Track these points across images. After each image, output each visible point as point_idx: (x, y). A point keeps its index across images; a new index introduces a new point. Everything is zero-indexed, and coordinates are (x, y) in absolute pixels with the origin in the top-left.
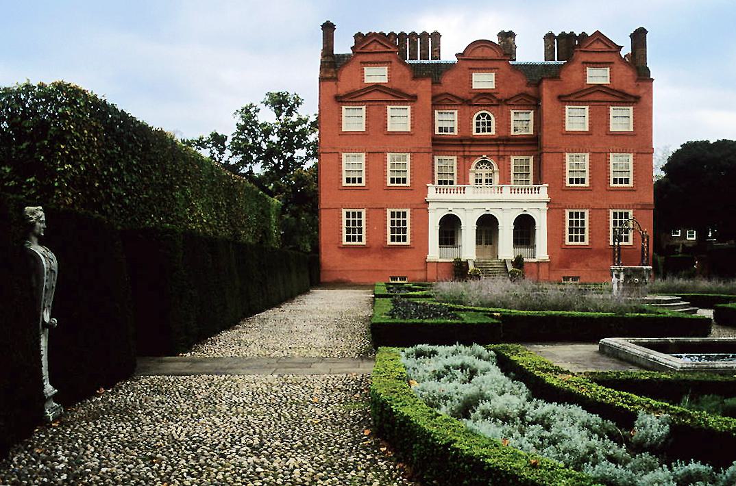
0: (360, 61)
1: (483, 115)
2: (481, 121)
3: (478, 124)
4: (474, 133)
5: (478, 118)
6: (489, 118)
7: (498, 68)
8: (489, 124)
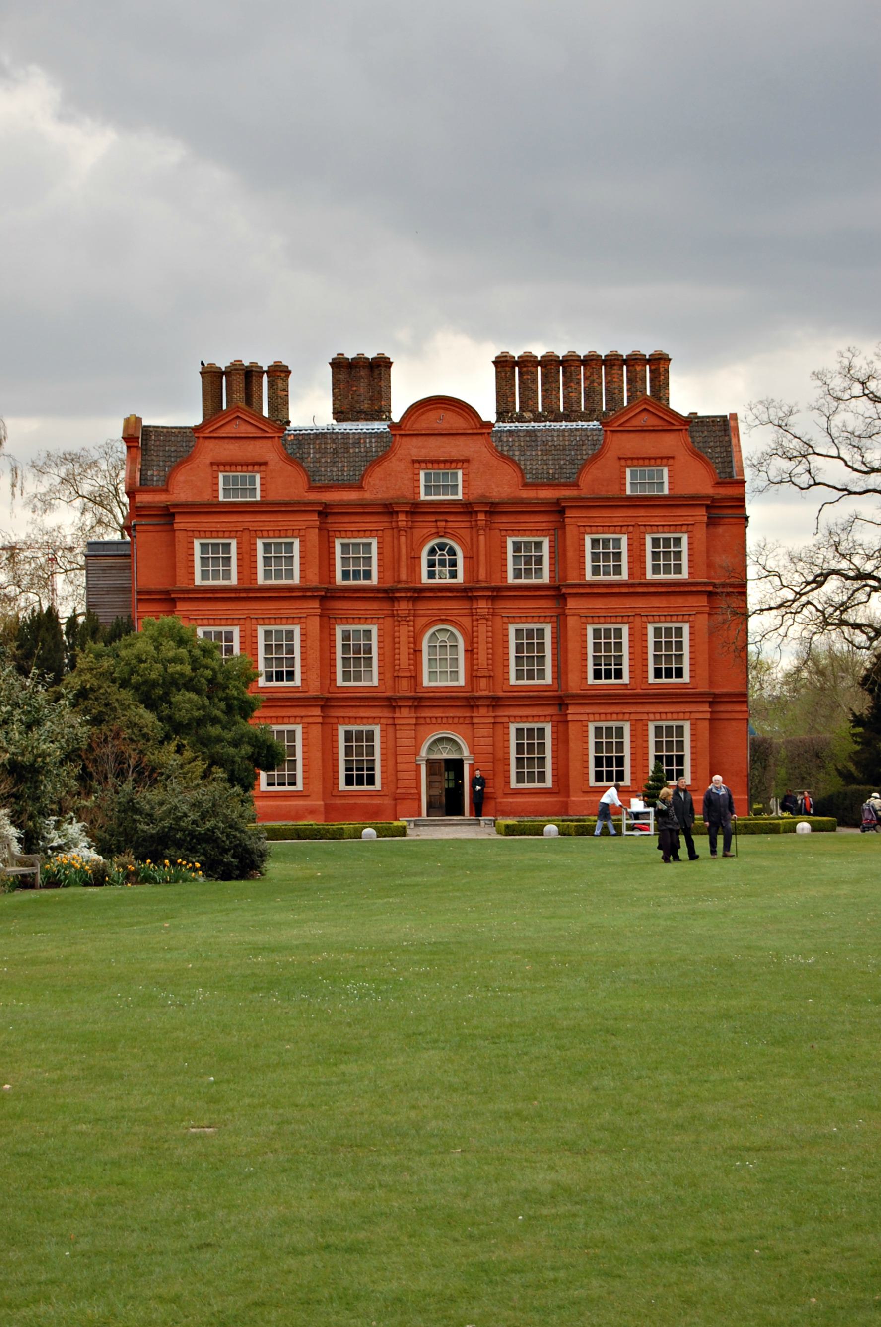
0: (208, 461)
1: (442, 547)
2: (437, 558)
3: (431, 564)
4: (425, 579)
5: (432, 552)
6: (452, 552)
7: (467, 461)
8: (453, 564)
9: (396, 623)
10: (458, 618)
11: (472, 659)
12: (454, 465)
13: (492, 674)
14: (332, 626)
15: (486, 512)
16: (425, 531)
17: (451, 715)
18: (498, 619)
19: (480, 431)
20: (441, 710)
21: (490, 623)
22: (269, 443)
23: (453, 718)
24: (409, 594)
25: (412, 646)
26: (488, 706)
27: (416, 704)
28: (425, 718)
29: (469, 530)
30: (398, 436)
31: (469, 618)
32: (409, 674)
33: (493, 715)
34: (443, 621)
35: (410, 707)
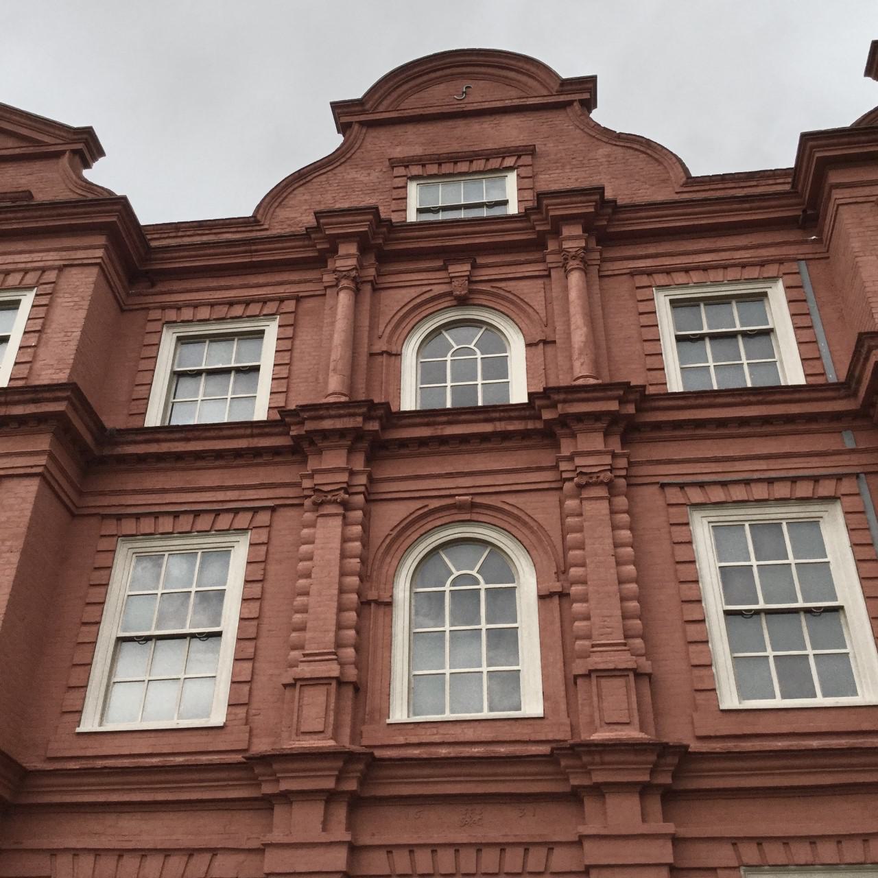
7: (531, 151)
9: (308, 516)
10: (511, 499)
11: (566, 621)
12: (495, 163)
13: (646, 665)
14: (104, 544)
15: (588, 224)
16: (413, 292)
17: (494, 834)
18: (649, 497)
19: (562, 98)
20: (452, 816)
21: (621, 502)
22: (51, 164)
23: (502, 847)
24: (349, 423)
25: (354, 581)
26: (644, 790)
27: (351, 785)
28: (389, 849)
29: (540, 282)
30: (356, 127)
31: (552, 498)
32: (333, 670)
33: (670, 828)
34: (470, 510)
35: (330, 797)
